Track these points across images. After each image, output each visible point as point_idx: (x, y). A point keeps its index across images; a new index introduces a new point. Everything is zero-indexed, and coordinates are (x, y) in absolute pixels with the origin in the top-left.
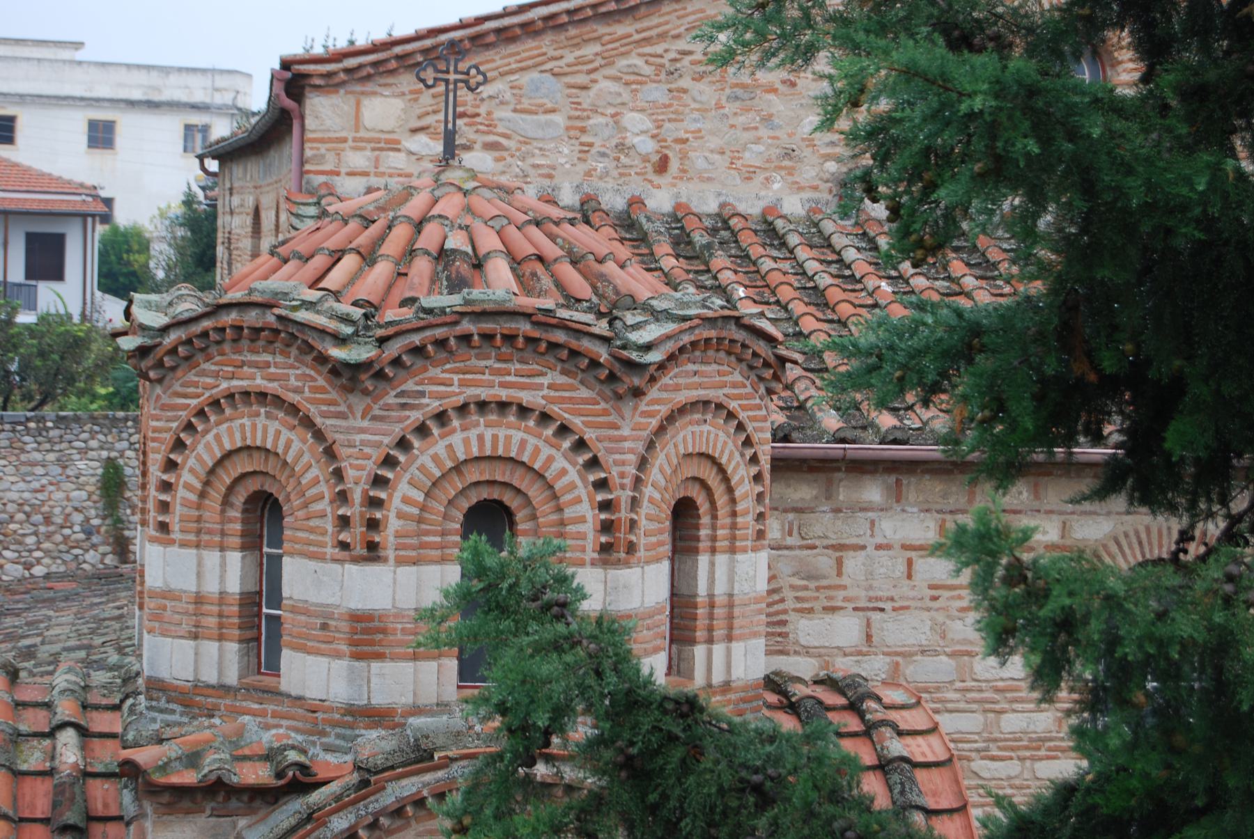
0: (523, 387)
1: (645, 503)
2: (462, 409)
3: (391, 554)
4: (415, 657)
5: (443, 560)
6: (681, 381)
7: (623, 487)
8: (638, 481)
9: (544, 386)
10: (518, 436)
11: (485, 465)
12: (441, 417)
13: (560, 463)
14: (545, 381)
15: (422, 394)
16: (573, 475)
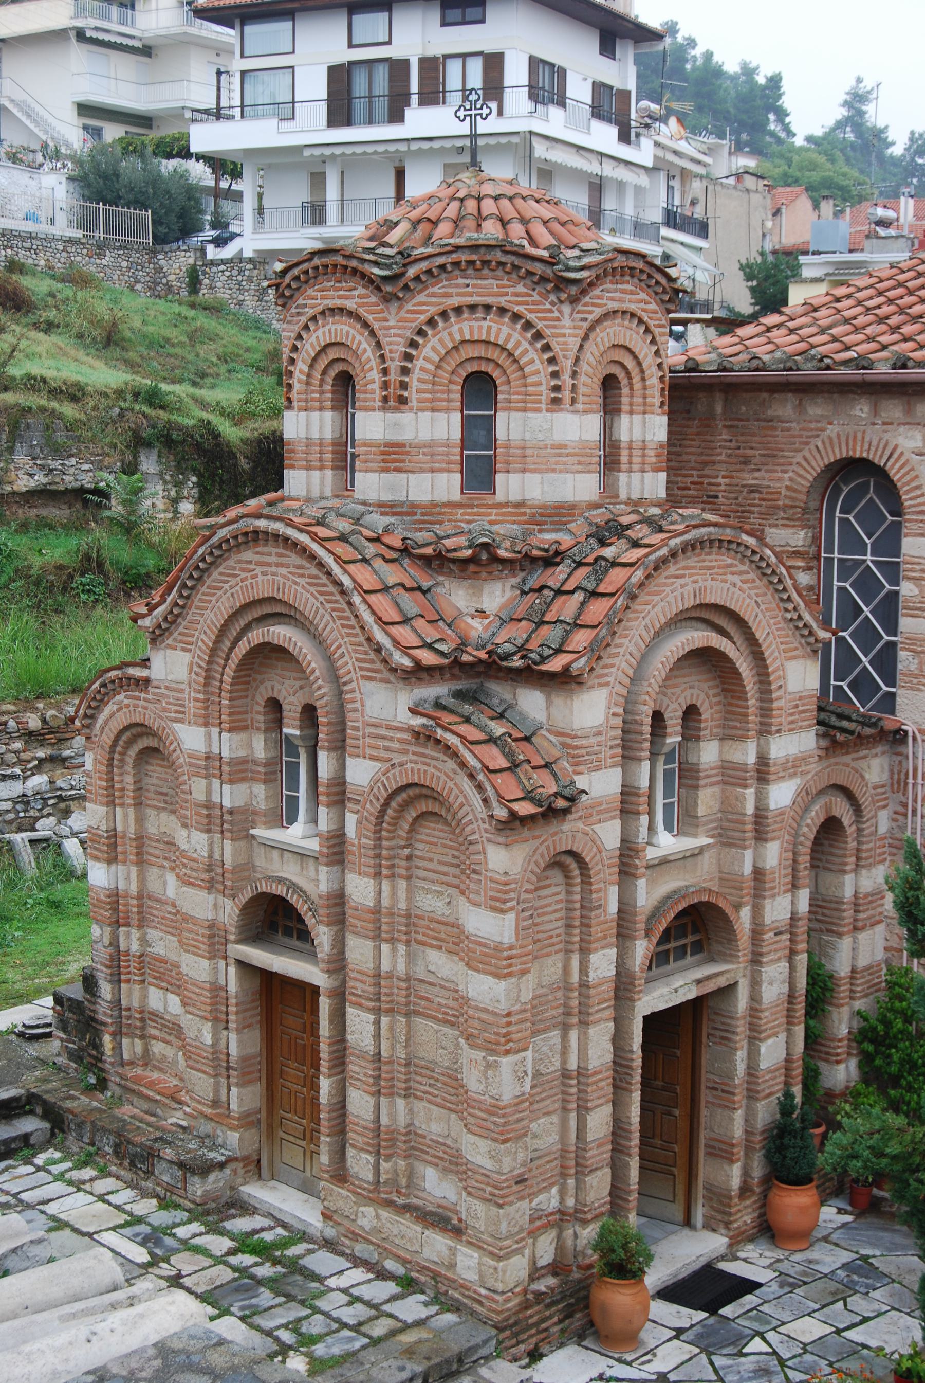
0: (346, 298)
1: (417, 370)
2: (323, 313)
3: (295, 404)
4: (308, 468)
5: (321, 409)
6: (454, 290)
7: (392, 359)
8: (408, 357)
9: (356, 297)
10: (346, 328)
11: (335, 349)
12: (314, 318)
13: (364, 345)
14: (356, 293)
15: (305, 306)
16: (369, 353)
